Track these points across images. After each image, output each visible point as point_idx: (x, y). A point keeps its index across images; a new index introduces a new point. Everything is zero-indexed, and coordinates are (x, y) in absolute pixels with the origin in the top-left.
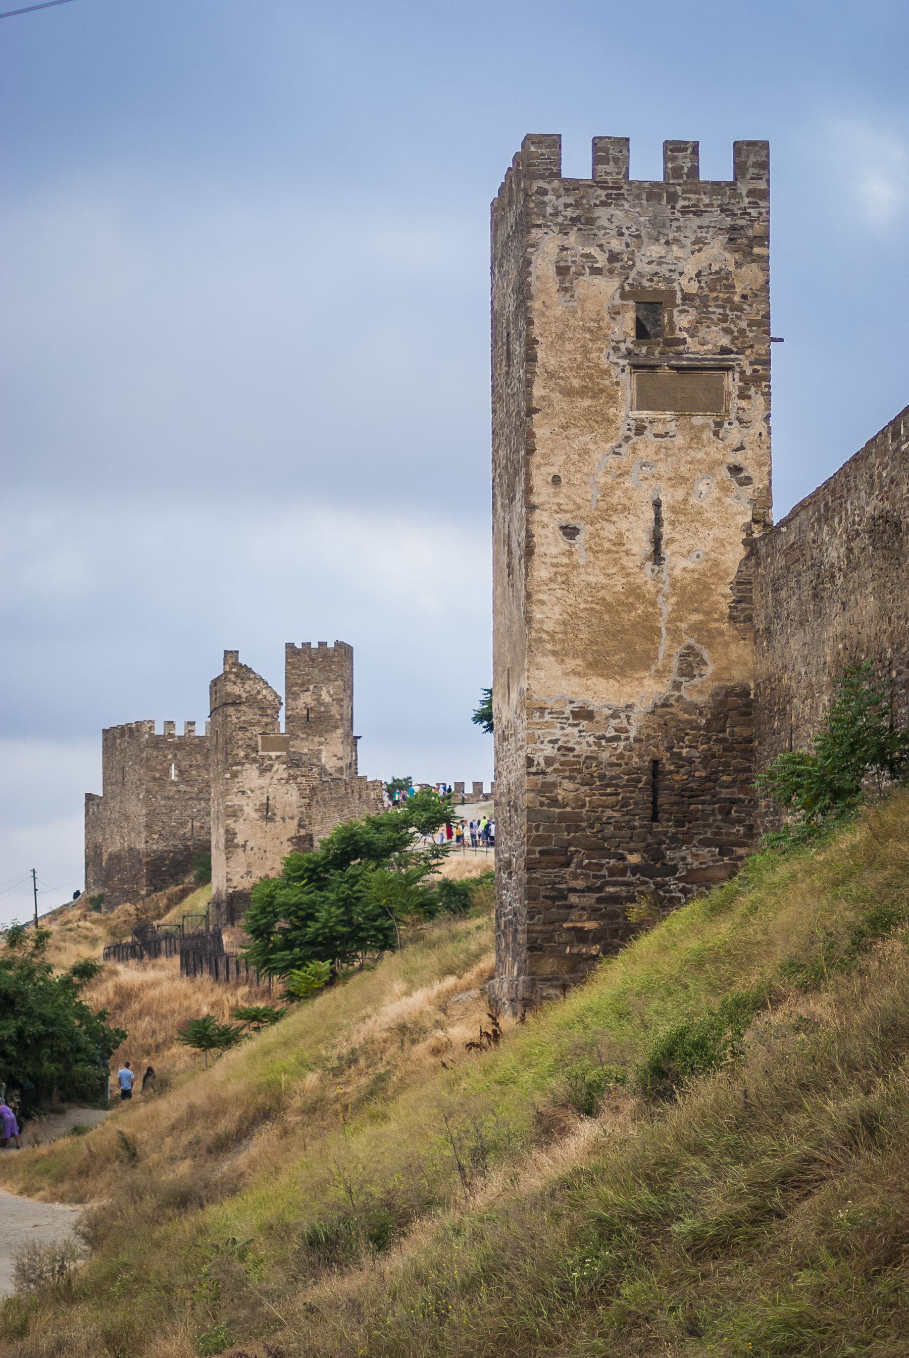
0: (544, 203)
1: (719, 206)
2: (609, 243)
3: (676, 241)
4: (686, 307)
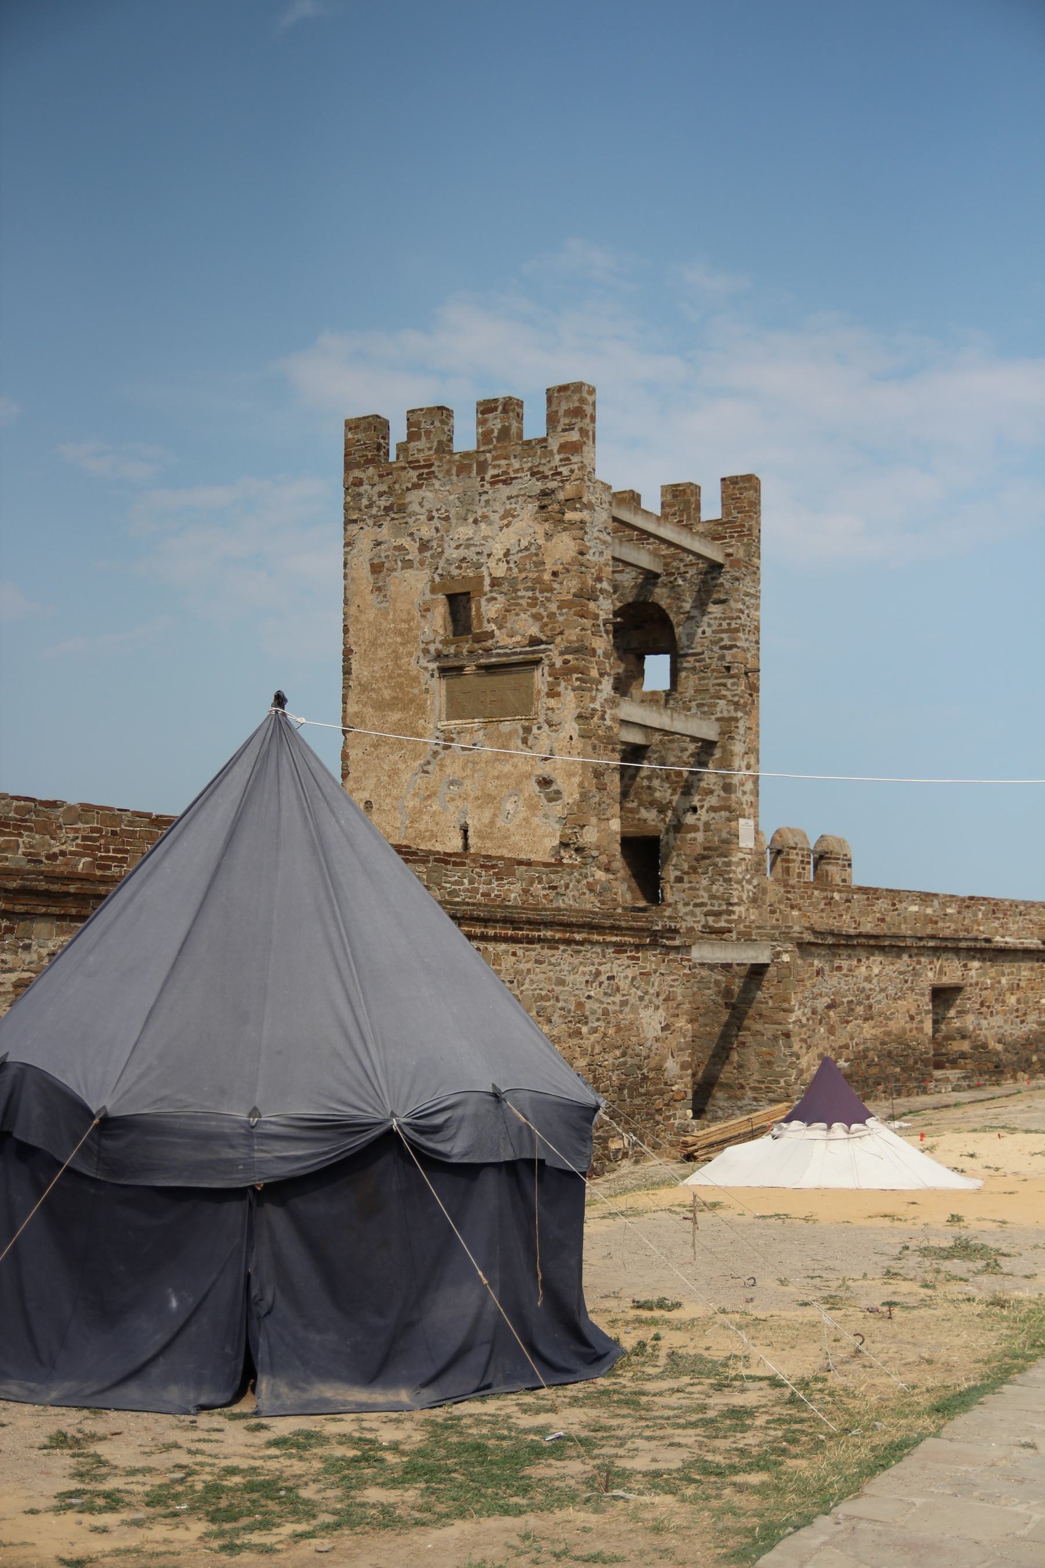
0: (360, 495)
1: (530, 469)
2: (419, 530)
3: (485, 517)
4: (494, 595)
